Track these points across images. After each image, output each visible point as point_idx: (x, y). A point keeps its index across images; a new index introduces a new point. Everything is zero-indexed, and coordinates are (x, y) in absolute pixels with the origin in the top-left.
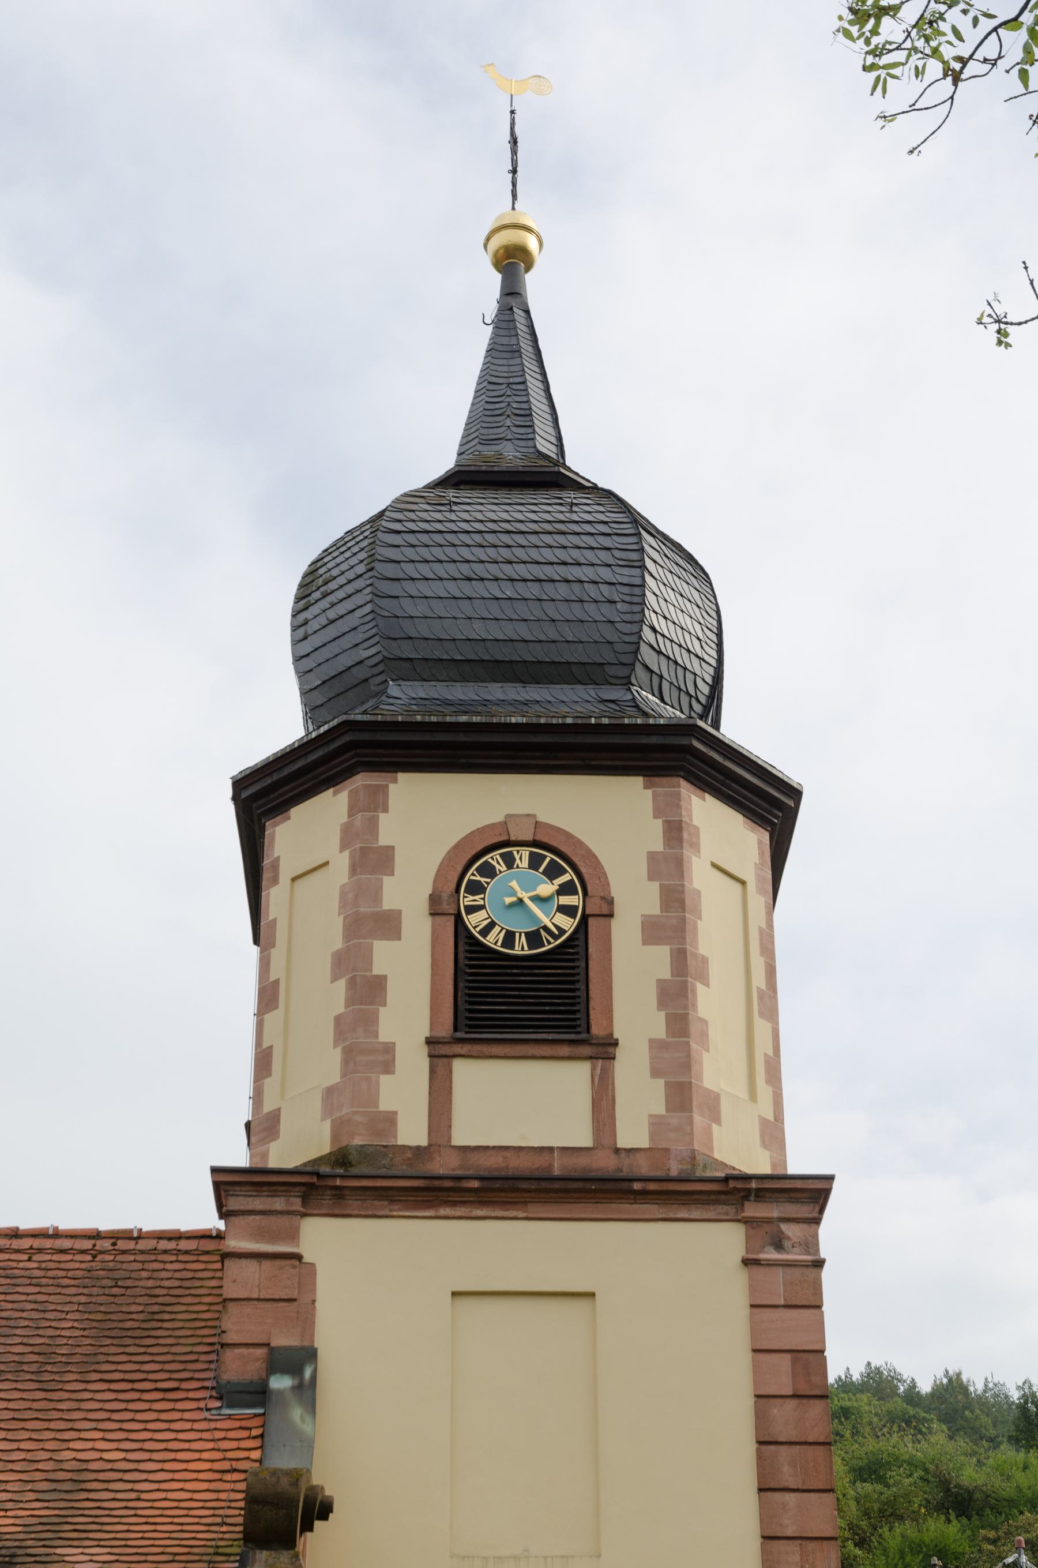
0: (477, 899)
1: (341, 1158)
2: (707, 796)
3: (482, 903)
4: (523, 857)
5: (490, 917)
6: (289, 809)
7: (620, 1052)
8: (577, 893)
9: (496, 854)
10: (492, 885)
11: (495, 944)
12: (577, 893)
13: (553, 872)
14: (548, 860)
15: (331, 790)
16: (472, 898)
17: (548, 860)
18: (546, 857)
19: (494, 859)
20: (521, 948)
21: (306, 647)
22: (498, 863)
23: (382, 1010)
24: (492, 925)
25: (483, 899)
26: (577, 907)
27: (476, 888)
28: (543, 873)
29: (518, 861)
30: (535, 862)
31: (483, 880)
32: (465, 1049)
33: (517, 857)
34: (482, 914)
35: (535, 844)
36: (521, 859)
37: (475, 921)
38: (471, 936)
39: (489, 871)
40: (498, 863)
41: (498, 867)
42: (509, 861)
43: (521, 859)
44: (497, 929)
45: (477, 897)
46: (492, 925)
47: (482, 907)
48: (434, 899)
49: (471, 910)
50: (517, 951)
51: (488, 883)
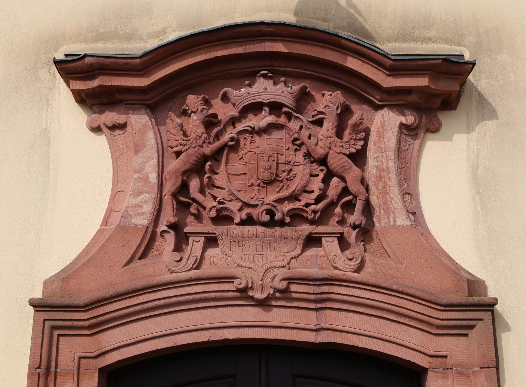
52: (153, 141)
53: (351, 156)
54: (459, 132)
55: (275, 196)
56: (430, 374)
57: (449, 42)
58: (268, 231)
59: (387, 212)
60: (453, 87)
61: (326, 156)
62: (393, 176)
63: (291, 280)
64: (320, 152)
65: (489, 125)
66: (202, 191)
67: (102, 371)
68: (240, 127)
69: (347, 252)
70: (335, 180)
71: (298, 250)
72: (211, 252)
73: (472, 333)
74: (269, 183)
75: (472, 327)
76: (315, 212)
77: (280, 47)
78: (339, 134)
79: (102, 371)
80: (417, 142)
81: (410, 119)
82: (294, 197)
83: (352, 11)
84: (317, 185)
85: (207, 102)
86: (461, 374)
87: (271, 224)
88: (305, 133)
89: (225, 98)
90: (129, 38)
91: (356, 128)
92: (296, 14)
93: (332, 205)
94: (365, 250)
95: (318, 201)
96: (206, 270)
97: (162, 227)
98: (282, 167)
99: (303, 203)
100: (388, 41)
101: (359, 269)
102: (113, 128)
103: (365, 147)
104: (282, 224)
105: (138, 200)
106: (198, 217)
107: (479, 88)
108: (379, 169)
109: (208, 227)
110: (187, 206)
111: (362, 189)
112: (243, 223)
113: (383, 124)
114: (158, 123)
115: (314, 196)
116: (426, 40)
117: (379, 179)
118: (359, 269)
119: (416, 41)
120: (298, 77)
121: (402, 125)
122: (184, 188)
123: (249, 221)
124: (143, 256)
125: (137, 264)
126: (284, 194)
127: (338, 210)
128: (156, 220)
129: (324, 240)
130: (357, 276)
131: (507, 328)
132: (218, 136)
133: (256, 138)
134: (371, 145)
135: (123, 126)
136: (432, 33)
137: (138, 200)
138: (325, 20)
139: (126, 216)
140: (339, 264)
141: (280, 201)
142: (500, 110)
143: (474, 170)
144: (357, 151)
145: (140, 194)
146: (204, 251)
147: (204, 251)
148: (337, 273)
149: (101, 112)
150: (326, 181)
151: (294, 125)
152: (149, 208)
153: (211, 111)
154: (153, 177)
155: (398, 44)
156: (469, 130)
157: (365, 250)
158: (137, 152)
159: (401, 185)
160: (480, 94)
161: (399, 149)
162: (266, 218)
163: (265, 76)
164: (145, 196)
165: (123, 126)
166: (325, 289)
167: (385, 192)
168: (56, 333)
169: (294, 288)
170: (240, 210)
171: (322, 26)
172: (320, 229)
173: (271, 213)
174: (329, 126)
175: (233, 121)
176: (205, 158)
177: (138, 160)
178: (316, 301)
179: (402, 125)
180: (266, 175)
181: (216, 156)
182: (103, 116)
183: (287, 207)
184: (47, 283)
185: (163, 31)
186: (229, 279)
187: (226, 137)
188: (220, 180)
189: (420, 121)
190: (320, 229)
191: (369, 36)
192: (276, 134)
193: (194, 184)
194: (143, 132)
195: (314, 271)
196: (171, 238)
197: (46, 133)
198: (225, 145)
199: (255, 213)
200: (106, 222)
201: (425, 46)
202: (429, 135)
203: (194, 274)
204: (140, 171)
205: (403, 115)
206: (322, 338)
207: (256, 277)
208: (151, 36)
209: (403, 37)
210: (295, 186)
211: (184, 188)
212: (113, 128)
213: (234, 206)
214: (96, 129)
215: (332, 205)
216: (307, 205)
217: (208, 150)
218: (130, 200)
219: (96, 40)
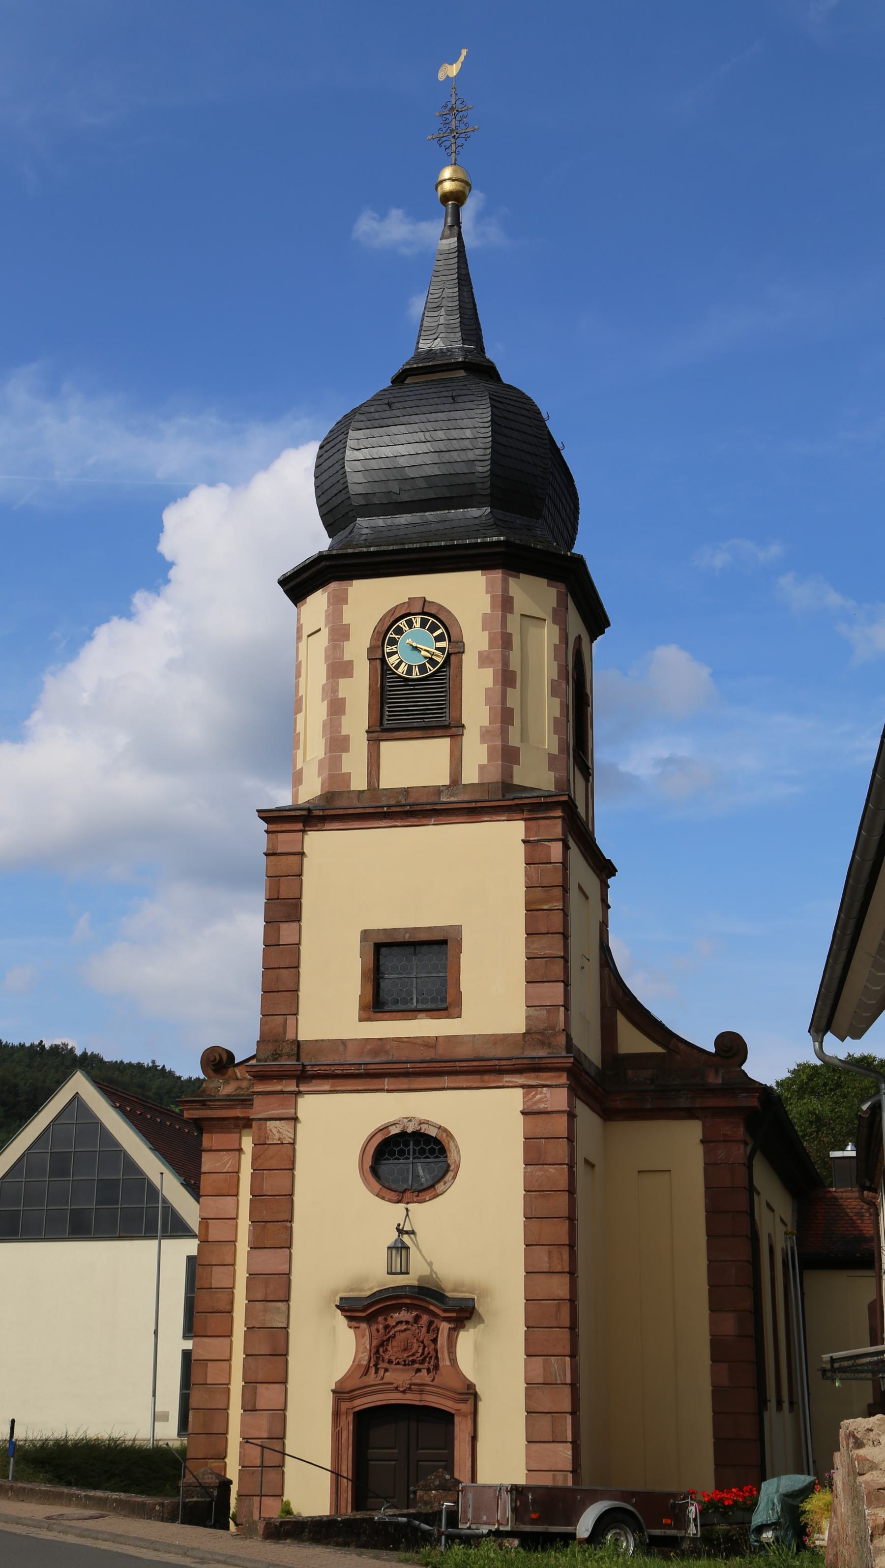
0: (393, 648)
1: (329, 796)
2: (521, 575)
3: (395, 650)
4: (417, 620)
5: (400, 658)
6: (306, 598)
7: (466, 732)
8: (445, 640)
9: (403, 621)
10: (401, 639)
11: (403, 673)
12: (445, 640)
13: (433, 629)
14: (430, 621)
15: (321, 590)
16: (390, 648)
17: (430, 621)
18: (429, 620)
19: (402, 623)
20: (416, 674)
21: (324, 499)
22: (404, 626)
23: (343, 717)
24: (401, 662)
25: (396, 648)
26: (446, 648)
27: (393, 642)
28: (427, 630)
29: (415, 624)
30: (423, 624)
31: (396, 637)
32: (385, 735)
33: (414, 621)
34: (395, 657)
35: (423, 613)
36: (416, 622)
37: (392, 661)
38: (391, 669)
39: (399, 631)
40: (404, 626)
41: (404, 628)
42: (410, 624)
43: (416, 622)
44: (403, 664)
45: (393, 647)
46: (401, 662)
47: (396, 653)
48: (370, 650)
49: (391, 654)
50: (414, 676)
51: (399, 638)
52: (368, 1334)
53: (432, 1340)
54: (472, 1328)
55: (406, 1355)
56: (455, 1416)
57: (470, 1293)
58: (404, 1367)
59: (443, 1360)
60: (468, 1315)
61: (423, 1341)
62: (446, 1347)
63: (411, 1384)
64: (421, 1339)
65: (481, 1326)
66: (384, 1352)
67: (354, 1413)
68: (396, 1329)
69: (430, 1374)
70: (427, 1348)
71: (414, 1374)
72: (387, 1374)
73: (469, 1402)
74: (405, 1350)
75: (468, 1400)
76: (419, 1360)
77: (408, 1301)
78: (428, 1332)
79: (354, 1413)
80: (456, 1333)
81: (453, 1326)
82: (413, 1355)
83: (437, 1280)
84: (420, 1350)
85: (386, 1319)
86: (464, 1416)
87: (405, 1365)
88: (417, 1331)
89: (392, 1317)
90: (361, 1290)
91: (433, 1330)
92: (418, 1281)
93: (426, 1357)
94: (436, 1373)
95: (421, 1356)
96: (385, 1381)
97: (371, 1365)
98: (409, 1345)
99: (416, 1357)
100: (449, 1292)
101: (433, 1381)
102: (355, 1328)
103: (437, 1337)
104: (408, 1365)
105: (363, 1355)
106: (383, 1361)
107: (479, 1311)
108: (441, 1344)
109: (386, 1365)
110: (379, 1357)
111: (434, 1353)
112: (396, 1364)
113: (443, 1328)
114: (370, 1326)
115: (420, 1354)
116: (462, 1292)
117: (441, 1348)
118: (433, 1381)
119: (459, 1292)
120: (416, 1309)
121: (450, 1328)
122: (377, 1352)
123: (398, 1363)
124: (365, 1375)
125: (364, 1378)
126: (409, 1354)
127: (428, 1359)
128: (369, 1362)
129: (422, 1370)
130: (431, 1383)
131: (481, 1400)
132: (389, 1333)
133: (401, 1334)
134: (439, 1335)
135: (359, 1328)
136: (464, 1289)
137: (363, 1355)
138: (428, 1283)
139: (360, 1361)
140: (426, 1379)
141: (408, 1356)
142: (485, 1320)
143: (476, 1342)
144: (434, 1338)
145: (363, 1353)
146: (384, 1373)
147: (384, 1373)
148: (425, 1382)
149: (351, 1321)
150: (424, 1349)
151: (414, 1328)
152: (367, 1358)
153: (387, 1323)
154: (368, 1347)
155: (452, 1294)
156: (475, 1327)
157: (436, 1373)
158: (363, 1338)
159: (448, 1349)
160: (479, 1314)
161: (449, 1336)
162: (403, 1363)
163: (405, 1310)
164: (366, 1354)
165: (359, 1328)
166: (422, 1387)
167: (443, 1353)
168: (339, 1400)
169: (412, 1387)
170: (396, 1359)
171: (427, 1286)
172: (421, 1366)
173: (405, 1361)
174: (424, 1330)
175: (394, 1327)
176: (384, 1341)
177: (363, 1340)
178: (420, 1391)
179: (450, 1328)
180: (403, 1348)
181: (388, 1340)
182: (352, 1323)
183: (410, 1359)
184: (336, 1383)
185: (372, 1288)
186: (392, 1384)
187: (391, 1333)
188: (389, 1348)
189: (457, 1325)
190: (421, 1366)
191: (443, 1290)
192: (408, 1332)
193: (381, 1350)
194: (365, 1330)
195: (418, 1381)
196: (373, 1370)
197: (334, 1328)
198: (390, 1337)
199: (400, 1361)
200: (354, 1362)
201: (460, 1294)
202: (462, 1330)
203: (381, 1382)
204: (364, 1344)
205: (450, 1324)
206: (422, 1403)
207: (401, 1383)
208: (368, 1290)
209: (454, 1290)
210: (413, 1351)
211: (377, 1352)
212: (355, 1328)
213: (393, 1358)
214: (350, 1327)
215: (426, 1357)
216: (417, 1358)
217: (385, 1338)
218: (361, 1355)
219: (350, 1291)
